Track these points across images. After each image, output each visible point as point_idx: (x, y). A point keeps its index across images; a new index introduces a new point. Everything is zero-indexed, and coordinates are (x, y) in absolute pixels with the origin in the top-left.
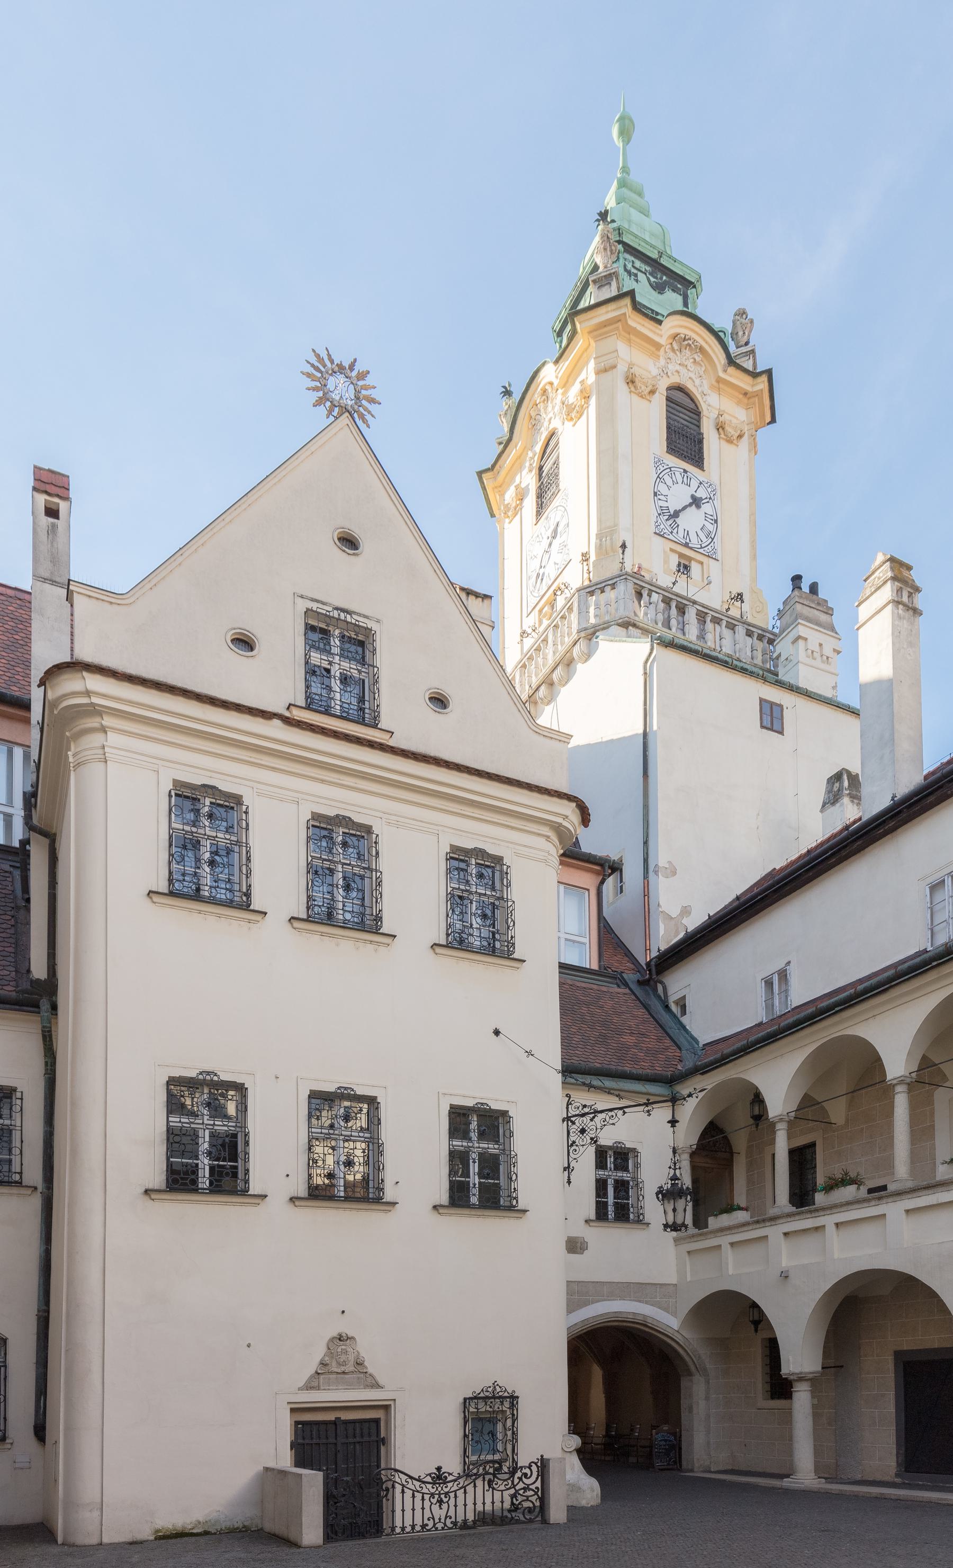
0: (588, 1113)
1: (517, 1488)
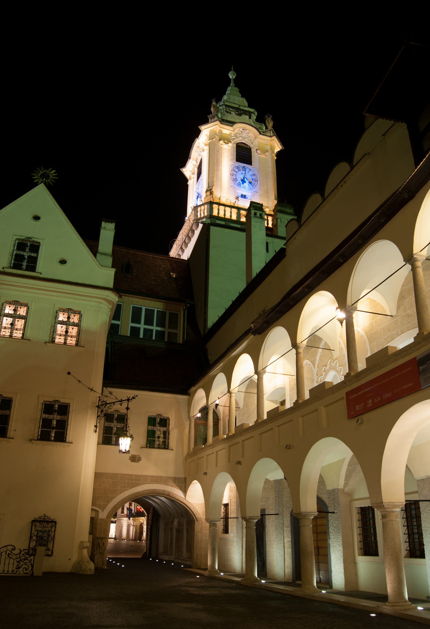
0: (104, 404)
1: (21, 558)
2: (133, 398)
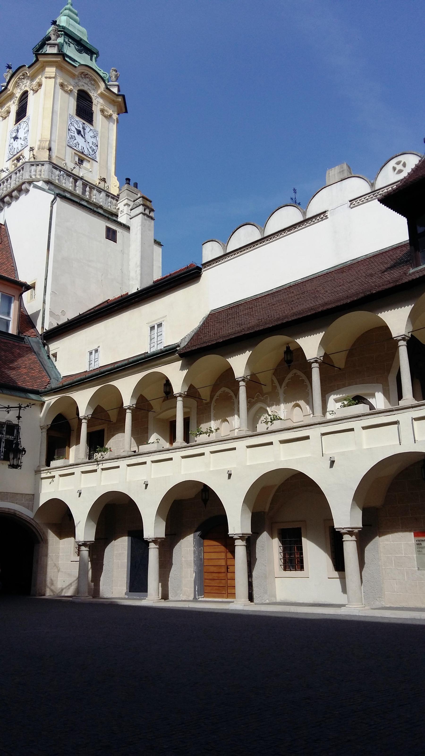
2: (28, 406)
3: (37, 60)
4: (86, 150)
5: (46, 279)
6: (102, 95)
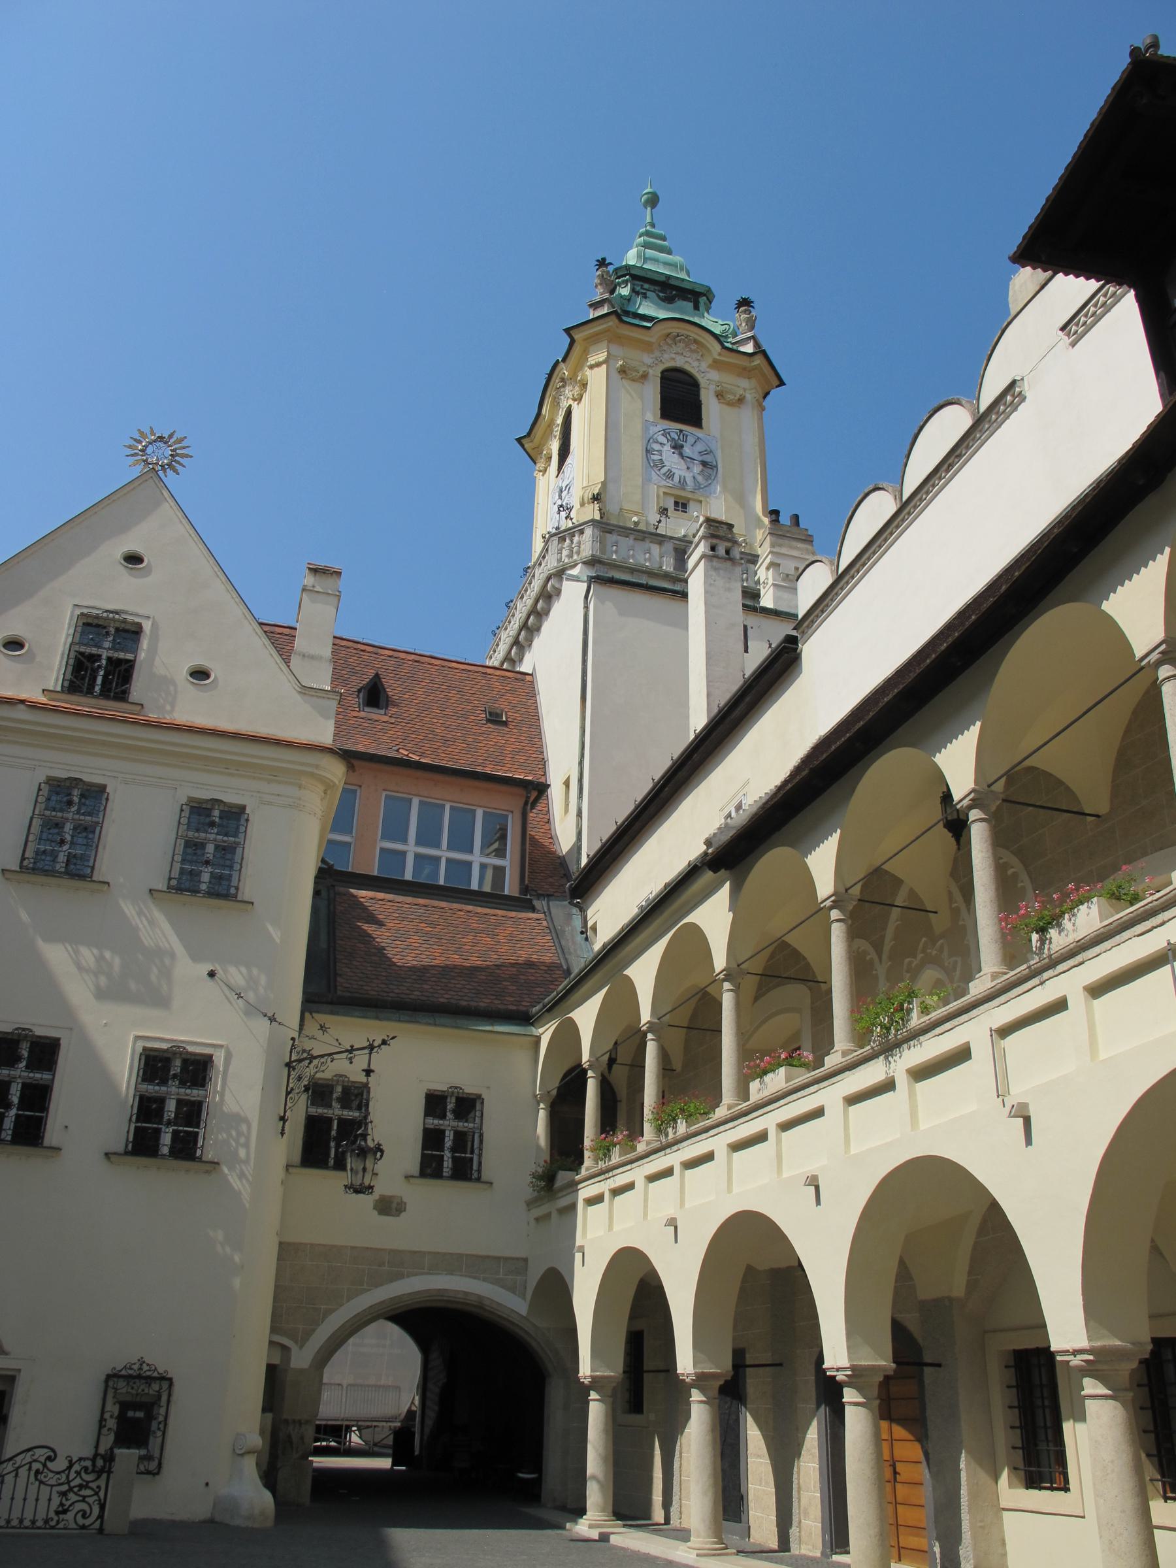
0: (306, 1059)
1: (72, 1484)
2: (384, 1042)
3: (572, 342)
4: (689, 481)
5: (581, 763)
6: (717, 365)
